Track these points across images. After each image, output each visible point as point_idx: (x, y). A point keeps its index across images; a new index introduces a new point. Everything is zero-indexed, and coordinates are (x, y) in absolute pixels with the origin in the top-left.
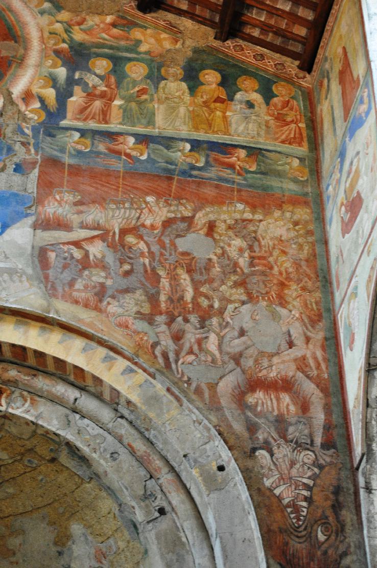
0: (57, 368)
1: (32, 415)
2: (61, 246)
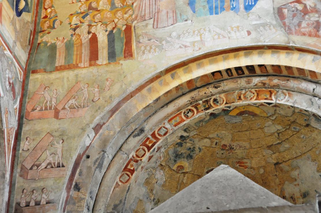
0: (300, 74)
1: (291, 102)
2: (290, 4)
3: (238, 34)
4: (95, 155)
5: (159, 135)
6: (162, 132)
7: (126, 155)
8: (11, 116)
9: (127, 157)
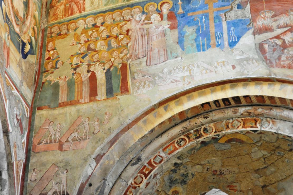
0: (282, 103)
1: (274, 129)
2: (270, 40)
3: (223, 67)
4: (96, 184)
5: (155, 163)
6: (157, 160)
7: (125, 182)
8: (19, 149)
9: (126, 184)
